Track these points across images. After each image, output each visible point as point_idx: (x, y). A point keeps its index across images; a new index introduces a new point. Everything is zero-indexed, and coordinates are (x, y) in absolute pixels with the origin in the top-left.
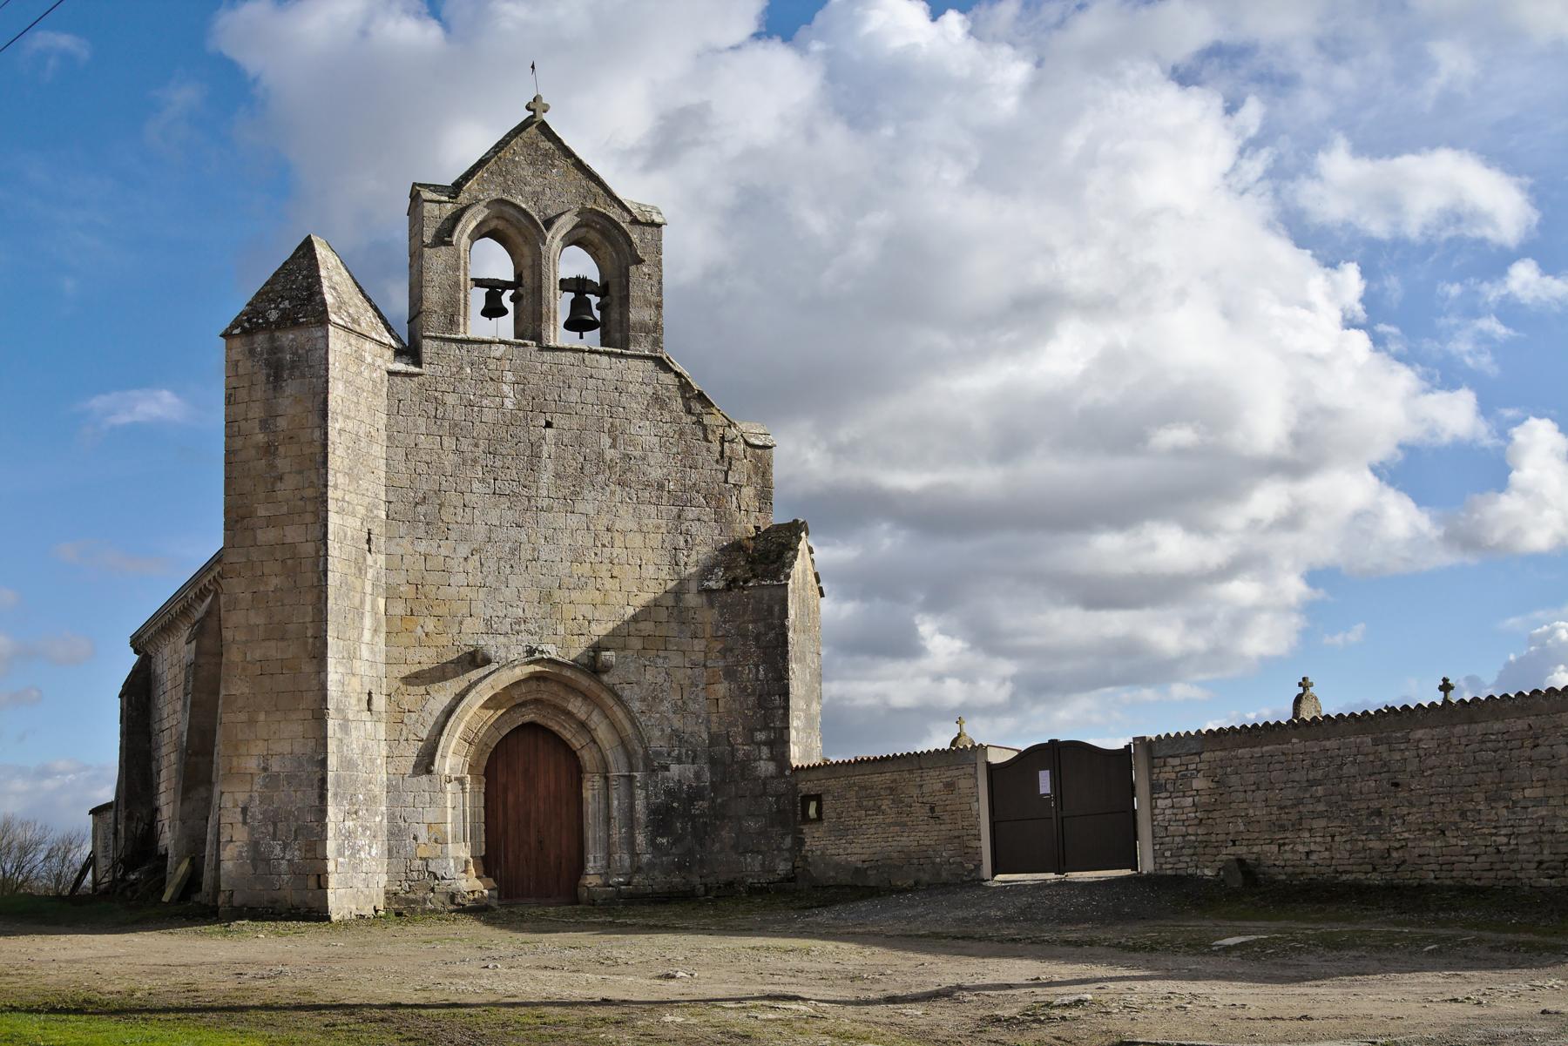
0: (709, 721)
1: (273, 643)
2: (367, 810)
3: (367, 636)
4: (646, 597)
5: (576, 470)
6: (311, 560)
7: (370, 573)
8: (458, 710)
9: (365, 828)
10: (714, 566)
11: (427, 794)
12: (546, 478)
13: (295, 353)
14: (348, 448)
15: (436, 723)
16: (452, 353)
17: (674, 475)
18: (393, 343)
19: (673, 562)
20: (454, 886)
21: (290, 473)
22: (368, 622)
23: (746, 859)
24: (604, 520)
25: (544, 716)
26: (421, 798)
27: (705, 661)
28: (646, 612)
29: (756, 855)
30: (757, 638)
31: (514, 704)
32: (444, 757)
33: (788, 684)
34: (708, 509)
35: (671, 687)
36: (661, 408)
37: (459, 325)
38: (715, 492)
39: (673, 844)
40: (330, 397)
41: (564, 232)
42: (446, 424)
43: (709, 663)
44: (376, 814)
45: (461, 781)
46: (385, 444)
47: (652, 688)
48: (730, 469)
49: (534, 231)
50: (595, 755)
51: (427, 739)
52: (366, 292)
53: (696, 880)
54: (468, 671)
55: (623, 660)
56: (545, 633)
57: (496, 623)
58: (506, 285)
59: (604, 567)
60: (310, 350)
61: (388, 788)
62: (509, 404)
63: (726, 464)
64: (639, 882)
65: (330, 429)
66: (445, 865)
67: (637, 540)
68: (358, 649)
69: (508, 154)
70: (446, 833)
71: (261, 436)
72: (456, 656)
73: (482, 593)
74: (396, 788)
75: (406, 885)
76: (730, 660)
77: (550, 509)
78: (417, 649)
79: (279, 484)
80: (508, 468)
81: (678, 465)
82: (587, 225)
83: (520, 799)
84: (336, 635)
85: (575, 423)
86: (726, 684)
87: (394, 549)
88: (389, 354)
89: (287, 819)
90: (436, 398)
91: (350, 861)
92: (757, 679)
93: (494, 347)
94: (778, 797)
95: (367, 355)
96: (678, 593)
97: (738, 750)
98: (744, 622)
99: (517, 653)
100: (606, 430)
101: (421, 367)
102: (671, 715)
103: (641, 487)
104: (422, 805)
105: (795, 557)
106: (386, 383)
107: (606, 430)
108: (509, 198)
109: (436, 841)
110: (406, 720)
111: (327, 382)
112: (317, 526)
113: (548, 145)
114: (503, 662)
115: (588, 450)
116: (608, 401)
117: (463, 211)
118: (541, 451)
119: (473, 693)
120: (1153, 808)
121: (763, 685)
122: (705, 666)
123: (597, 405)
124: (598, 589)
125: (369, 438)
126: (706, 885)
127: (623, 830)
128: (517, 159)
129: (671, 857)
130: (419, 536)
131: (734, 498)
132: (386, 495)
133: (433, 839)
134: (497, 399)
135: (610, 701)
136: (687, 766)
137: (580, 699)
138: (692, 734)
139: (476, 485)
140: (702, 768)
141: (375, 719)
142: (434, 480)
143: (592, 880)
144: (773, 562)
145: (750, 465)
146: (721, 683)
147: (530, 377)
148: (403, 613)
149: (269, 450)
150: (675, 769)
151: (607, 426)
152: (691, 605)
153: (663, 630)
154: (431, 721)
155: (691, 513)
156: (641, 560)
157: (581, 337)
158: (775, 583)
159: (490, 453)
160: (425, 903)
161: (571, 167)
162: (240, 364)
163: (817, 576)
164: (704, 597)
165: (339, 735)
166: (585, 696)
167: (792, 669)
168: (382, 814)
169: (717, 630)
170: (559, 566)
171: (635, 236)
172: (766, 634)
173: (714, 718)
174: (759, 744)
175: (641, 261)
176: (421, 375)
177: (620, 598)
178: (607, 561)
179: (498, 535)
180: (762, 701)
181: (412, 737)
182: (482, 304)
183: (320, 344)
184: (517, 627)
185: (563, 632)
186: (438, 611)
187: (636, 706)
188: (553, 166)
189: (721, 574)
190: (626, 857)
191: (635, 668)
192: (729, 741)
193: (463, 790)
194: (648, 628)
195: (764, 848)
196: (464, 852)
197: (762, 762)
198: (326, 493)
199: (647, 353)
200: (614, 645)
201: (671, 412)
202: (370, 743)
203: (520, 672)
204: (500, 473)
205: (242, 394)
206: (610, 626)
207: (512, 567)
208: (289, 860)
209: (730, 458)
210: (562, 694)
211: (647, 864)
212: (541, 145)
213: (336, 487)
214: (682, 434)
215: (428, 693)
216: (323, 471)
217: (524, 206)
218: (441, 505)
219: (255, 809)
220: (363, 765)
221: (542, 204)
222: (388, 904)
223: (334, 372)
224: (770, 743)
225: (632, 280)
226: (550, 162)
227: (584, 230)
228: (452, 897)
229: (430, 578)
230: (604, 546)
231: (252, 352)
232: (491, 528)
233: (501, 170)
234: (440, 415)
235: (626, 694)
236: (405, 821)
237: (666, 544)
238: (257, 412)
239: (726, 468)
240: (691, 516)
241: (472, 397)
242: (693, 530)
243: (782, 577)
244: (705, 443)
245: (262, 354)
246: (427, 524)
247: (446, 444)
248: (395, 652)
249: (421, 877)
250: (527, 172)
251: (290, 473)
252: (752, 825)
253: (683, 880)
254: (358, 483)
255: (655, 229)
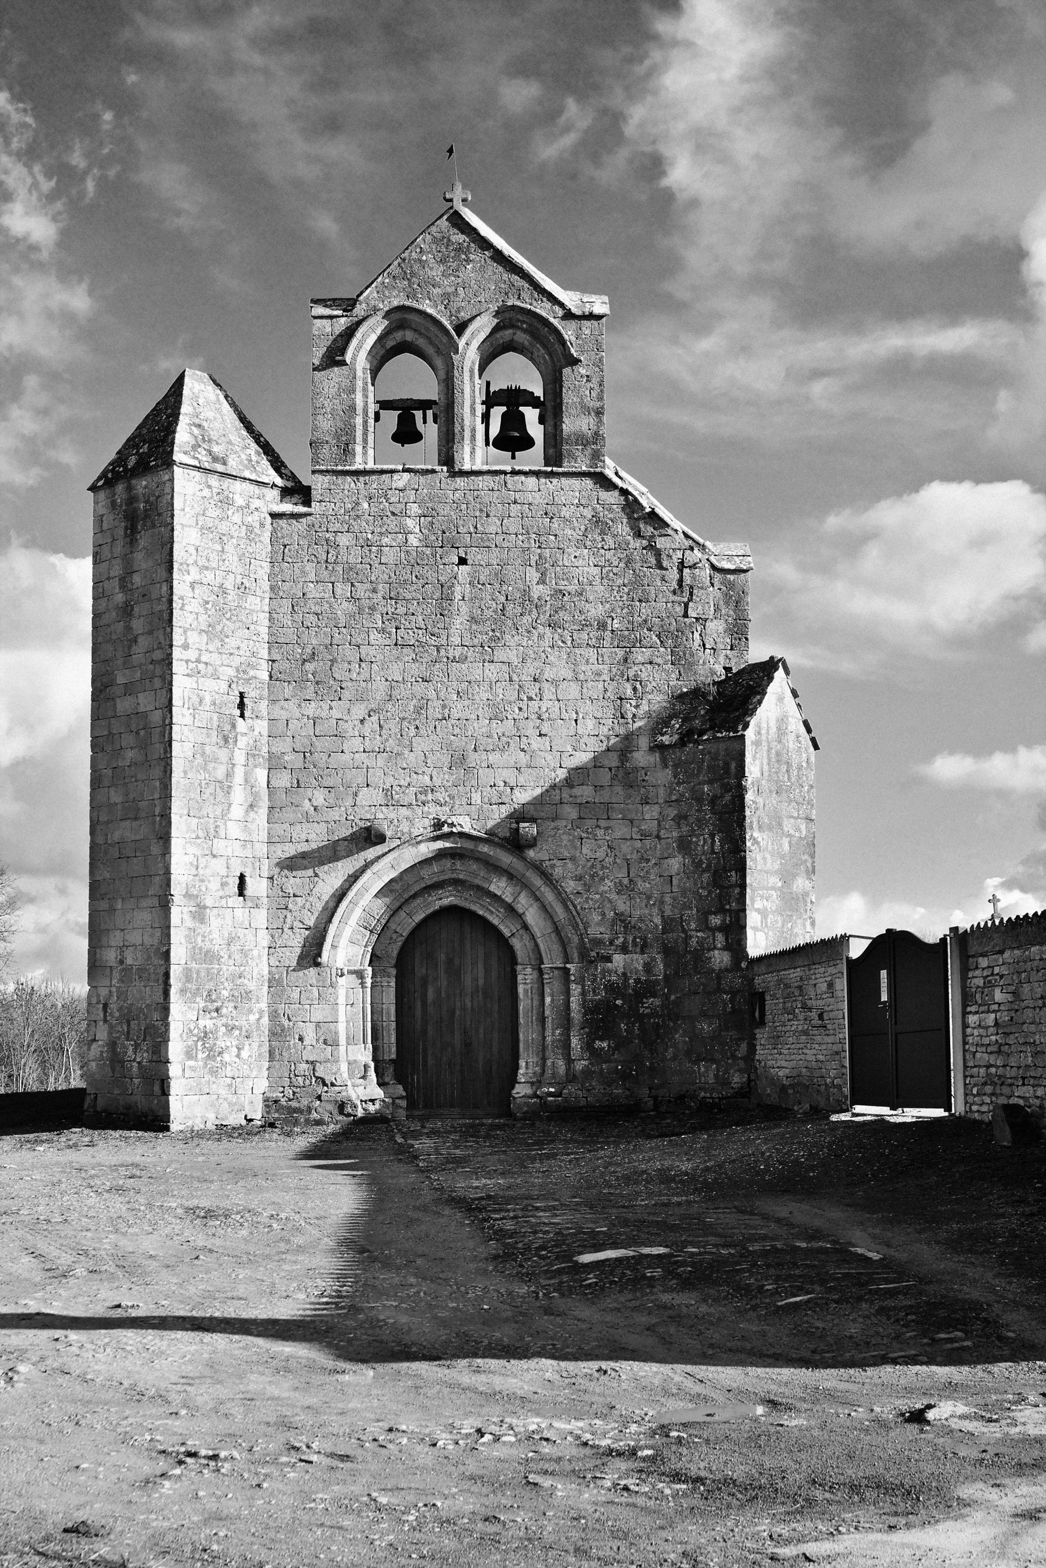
0: (662, 902)
1: (127, 823)
2: (236, 1007)
3: (237, 811)
4: (583, 758)
5: (495, 611)
6: (158, 730)
7: (242, 742)
8: (351, 894)
9: (230, 1029)
10: (671, 717)
11: (315, 989)
12: (459, 623)
13: (146, 502)
14: (207, 603)
15: (324, 909)
16: (347, 487)
17: (619, 611)
18: (279, 481)
19: (618, 714)
20: (344, 1094)
21: (143, 634)
22: (239, 796)
23: (699, 1069)
24: (531, 669)
25: (466, 899)
26: (307, 994)
27: (659, 831)
28: (577, 776)
29: (709, 1064)
30: (713, 801)
31: (423, 885)
32: (334, 947)
33: (745, 857)
34: (662, 649)
35: (615, 863)
36: (602, 533)
37: (354, 455)
38: (672, 628)
39: (617, 1048)
40: (176, 546)
41: (482, 336)
42: (339, 568)
43: (662, 833)
44: (250, 1011)
45: (360, 974)
46: (267, 595)
47: (590, 864)
48: (690, 600)
49: (445, 339)
50: (527, 944)
51: (316, 926)
52: (258, 427)
53: (644, 1092)
54: (363, 849)
55: (552, 833)
56: (457, 802)
57: (397, 793)
58: (425, 405)
59: (531, 724)
60: (159, 497)
61: (270, 981)
62: (413, 540)
63: (686, 594)
64: (570, 1093)
65: (175, 583)
66: (334, 1070)
67: (572, 690)
68: (222, 827)
69: (413, 254)
70: (336, 1033)
71: (121, 595)
72: (350, 831)
73: (381, 760)
74: (279, 982)
75: (289, 1092)
76: (685, 829)
77: (463, 659)
78: (304, 825)
79: (134, 647)
80: (413, 614)
81: (625, 599)
82: (513, 326)
83: (443, 995)
84: (186, 812)
85: (494, 556)
86: (680, 858)
87: (278, 712)
88: (276, 493)
89: (138, 1019)
90: (327, 540)
91: (206, 1064)
92: (713, 852)
93: (396, 476)
94: (734, 993)
95: (236, 497)
96: (625, 746)
97: (691, 937)
98: (699, 784)
99: (422, 826)
100: (533, 563)
101: (310, 506)
102: (613, 896)
103: (577, 628)
104: (309, 1002)
105: (760, 702)
106: (268, 527)
107: (533, 563)
108: (415, 305)
109: (325, 1042)
110: (290, 906)
111: (172, 530)
112: (164, 692)
113: (460, 238)
114: (406, 837)
115: (510, 588)
116: (535, 530)
117: (359, 323)
118: (453, 593)
119: (368, 874)
120: (965, 1026)
121: (718, 858)
122: (658, 837)
123: (522, 534)
124: (523, 750)
125: (242, 590)
126: (655, 1098)
127: (558, 1032)
128: (424, 258)
129: (612, 1065)
130: (308, 698)
131: (697, 635)
132: (269, 653)
133: (321, 1041)
134: (400, 536)
135: (537, 881)
136: (635, 956)
137: (505, 879)
138: (641, 919)
139: (374, 636)
140: (654, 959)
141: (250, 905)
142: (324, 633)
143: (521, 1090)
144: (737, 710)
145: (719, 594)
146: (674, 857)
147: (439, 507)
148: (289, 785)
149: (127, 611)
150: (619, 960)
151: (534, 559)
152: (641, 765)
153: (605, 796)
154: (319, 906)
155: (640, 655)
156: (577, 713)
157: (513, 457)
158: (731, 734)
159: (391, 598)
160: (310, 1113)
161: (489, 261)
162: (104, 518)
163: (806, 724)
164: (657, 755)
165: (189, 923)
166: (511, 876)
167: (756, 842)
168: (261, 1012)
169: (671, 794)
170: (475, 724)
171: (570, 333)
172: (722, 797)
173: (668, 899)
174: (713, 930)
175: (576, 362)
176: (310, 515)
177: (552, 759)
178: (535, 716)
179: (400, 692)
180: (718, 878)
181: (297, 924)
182: (393, 428)
183: (167, 490)
184: (423, 797)
185: (479, 802)
186: (328, 782)
187: (570, 886)
188: (468, 261)
189: (677, 726)
190: (561, 1063)
191: (569, 841)
192: (682, 926)
193: (363, 984)
194: (586, 793)
195: (718, 1056)
196: (364, 1055)
197: (716, 952)
198: (171, 654)
199: (584, 468)
200: (542, 814)
201: (614, 536)
202: (241, 932)
203: (427, 849)
204: (403, 621)
205: (106, 553)
206: (538, 791)
207: (417, 728)
208: (139, 1063)
209: (691, 587)
210: (482, 874)
211: (583, 1071)
212: (453, 238)
213: (186, 647)
214: (629, 561)
215: (316, 875)
216: (168, 629)
217: (430, 311)
218: (333, 661)
219: (113, 1007)
220: (230, 957)
221: (454, 306)
222: (268, 1113)
223: (179, 519)
224: (724, 929)
225: (565, 384)
226: (463, 256)
227: (510, 332)
228: (341, 1107)
229: (319, 744)
230: (530, 699)
231: (113, 504)
232: (392, 684)
233: (405, 273)
234: (331, 559)
235: (558, 872)
236: (290, 1020)
237: (609, 694)
238: (117, 570)
239: (686, 600)
240: (640, 659)
241: (370, 536)
242: (643, 676)
243: (740, 727)
244: (659, 571)
245: (121, 506)
246: (317, 683)
247: (338, 591)
248: (279, 829)
249: (307, 1082)
250: (436, 272)
251: (143, 634)
252: (705, 1027)
253: (628, 1093)
254: (222, 640)
255: (595, 323)
